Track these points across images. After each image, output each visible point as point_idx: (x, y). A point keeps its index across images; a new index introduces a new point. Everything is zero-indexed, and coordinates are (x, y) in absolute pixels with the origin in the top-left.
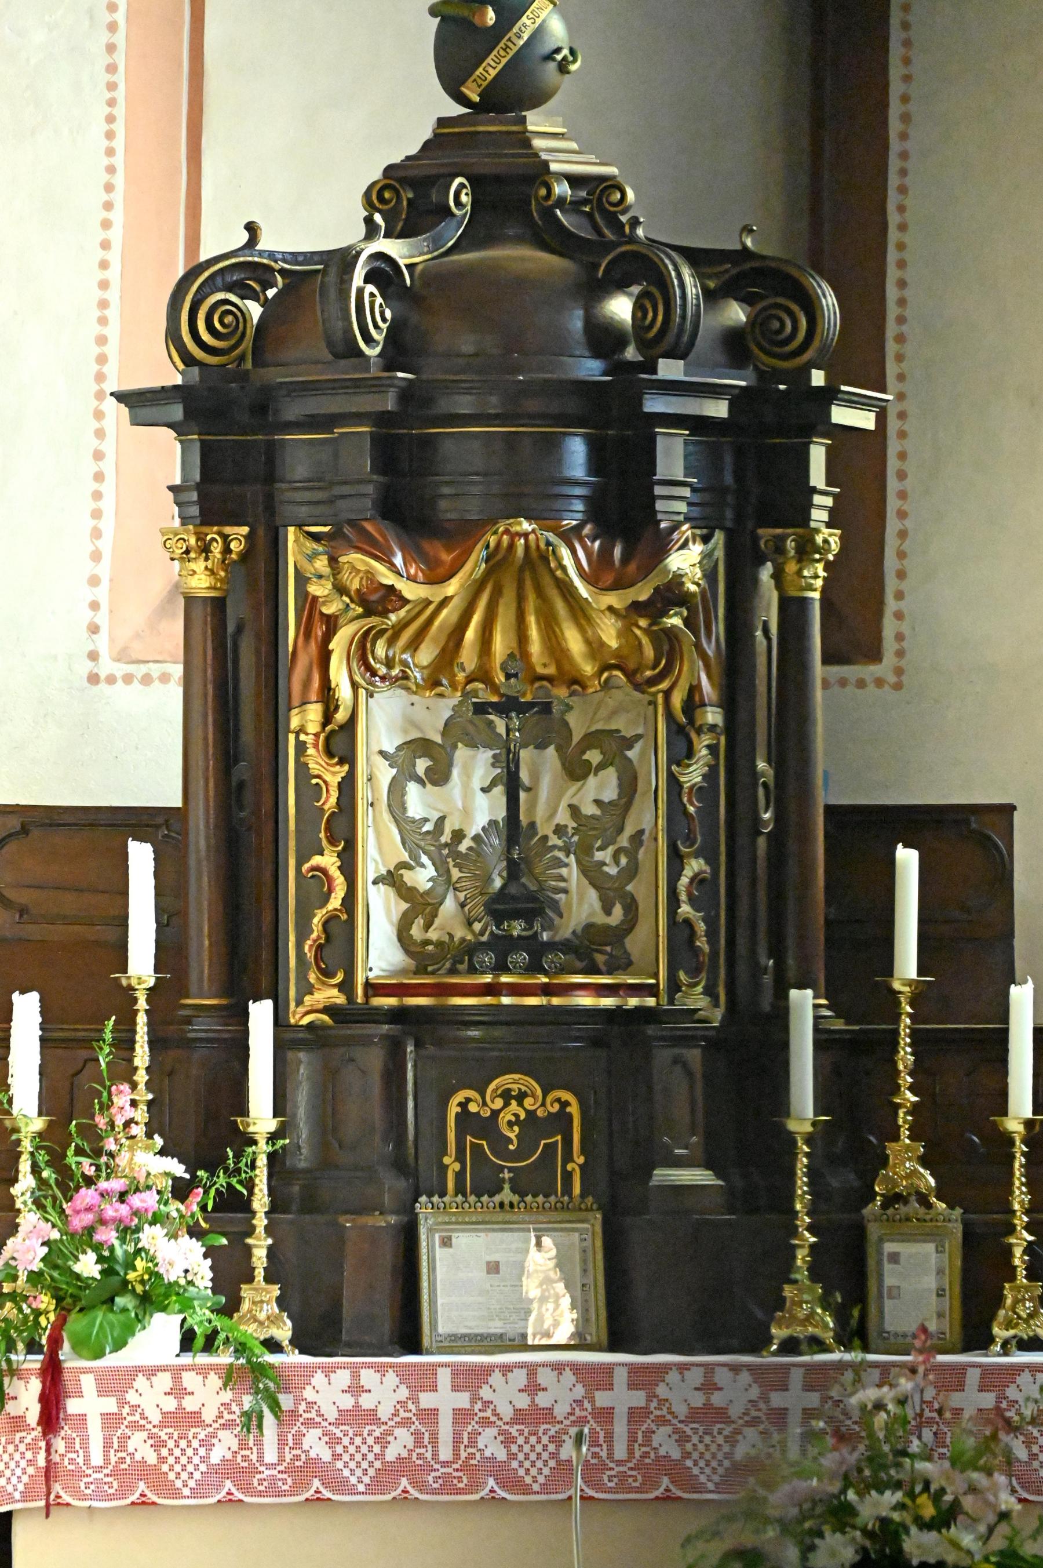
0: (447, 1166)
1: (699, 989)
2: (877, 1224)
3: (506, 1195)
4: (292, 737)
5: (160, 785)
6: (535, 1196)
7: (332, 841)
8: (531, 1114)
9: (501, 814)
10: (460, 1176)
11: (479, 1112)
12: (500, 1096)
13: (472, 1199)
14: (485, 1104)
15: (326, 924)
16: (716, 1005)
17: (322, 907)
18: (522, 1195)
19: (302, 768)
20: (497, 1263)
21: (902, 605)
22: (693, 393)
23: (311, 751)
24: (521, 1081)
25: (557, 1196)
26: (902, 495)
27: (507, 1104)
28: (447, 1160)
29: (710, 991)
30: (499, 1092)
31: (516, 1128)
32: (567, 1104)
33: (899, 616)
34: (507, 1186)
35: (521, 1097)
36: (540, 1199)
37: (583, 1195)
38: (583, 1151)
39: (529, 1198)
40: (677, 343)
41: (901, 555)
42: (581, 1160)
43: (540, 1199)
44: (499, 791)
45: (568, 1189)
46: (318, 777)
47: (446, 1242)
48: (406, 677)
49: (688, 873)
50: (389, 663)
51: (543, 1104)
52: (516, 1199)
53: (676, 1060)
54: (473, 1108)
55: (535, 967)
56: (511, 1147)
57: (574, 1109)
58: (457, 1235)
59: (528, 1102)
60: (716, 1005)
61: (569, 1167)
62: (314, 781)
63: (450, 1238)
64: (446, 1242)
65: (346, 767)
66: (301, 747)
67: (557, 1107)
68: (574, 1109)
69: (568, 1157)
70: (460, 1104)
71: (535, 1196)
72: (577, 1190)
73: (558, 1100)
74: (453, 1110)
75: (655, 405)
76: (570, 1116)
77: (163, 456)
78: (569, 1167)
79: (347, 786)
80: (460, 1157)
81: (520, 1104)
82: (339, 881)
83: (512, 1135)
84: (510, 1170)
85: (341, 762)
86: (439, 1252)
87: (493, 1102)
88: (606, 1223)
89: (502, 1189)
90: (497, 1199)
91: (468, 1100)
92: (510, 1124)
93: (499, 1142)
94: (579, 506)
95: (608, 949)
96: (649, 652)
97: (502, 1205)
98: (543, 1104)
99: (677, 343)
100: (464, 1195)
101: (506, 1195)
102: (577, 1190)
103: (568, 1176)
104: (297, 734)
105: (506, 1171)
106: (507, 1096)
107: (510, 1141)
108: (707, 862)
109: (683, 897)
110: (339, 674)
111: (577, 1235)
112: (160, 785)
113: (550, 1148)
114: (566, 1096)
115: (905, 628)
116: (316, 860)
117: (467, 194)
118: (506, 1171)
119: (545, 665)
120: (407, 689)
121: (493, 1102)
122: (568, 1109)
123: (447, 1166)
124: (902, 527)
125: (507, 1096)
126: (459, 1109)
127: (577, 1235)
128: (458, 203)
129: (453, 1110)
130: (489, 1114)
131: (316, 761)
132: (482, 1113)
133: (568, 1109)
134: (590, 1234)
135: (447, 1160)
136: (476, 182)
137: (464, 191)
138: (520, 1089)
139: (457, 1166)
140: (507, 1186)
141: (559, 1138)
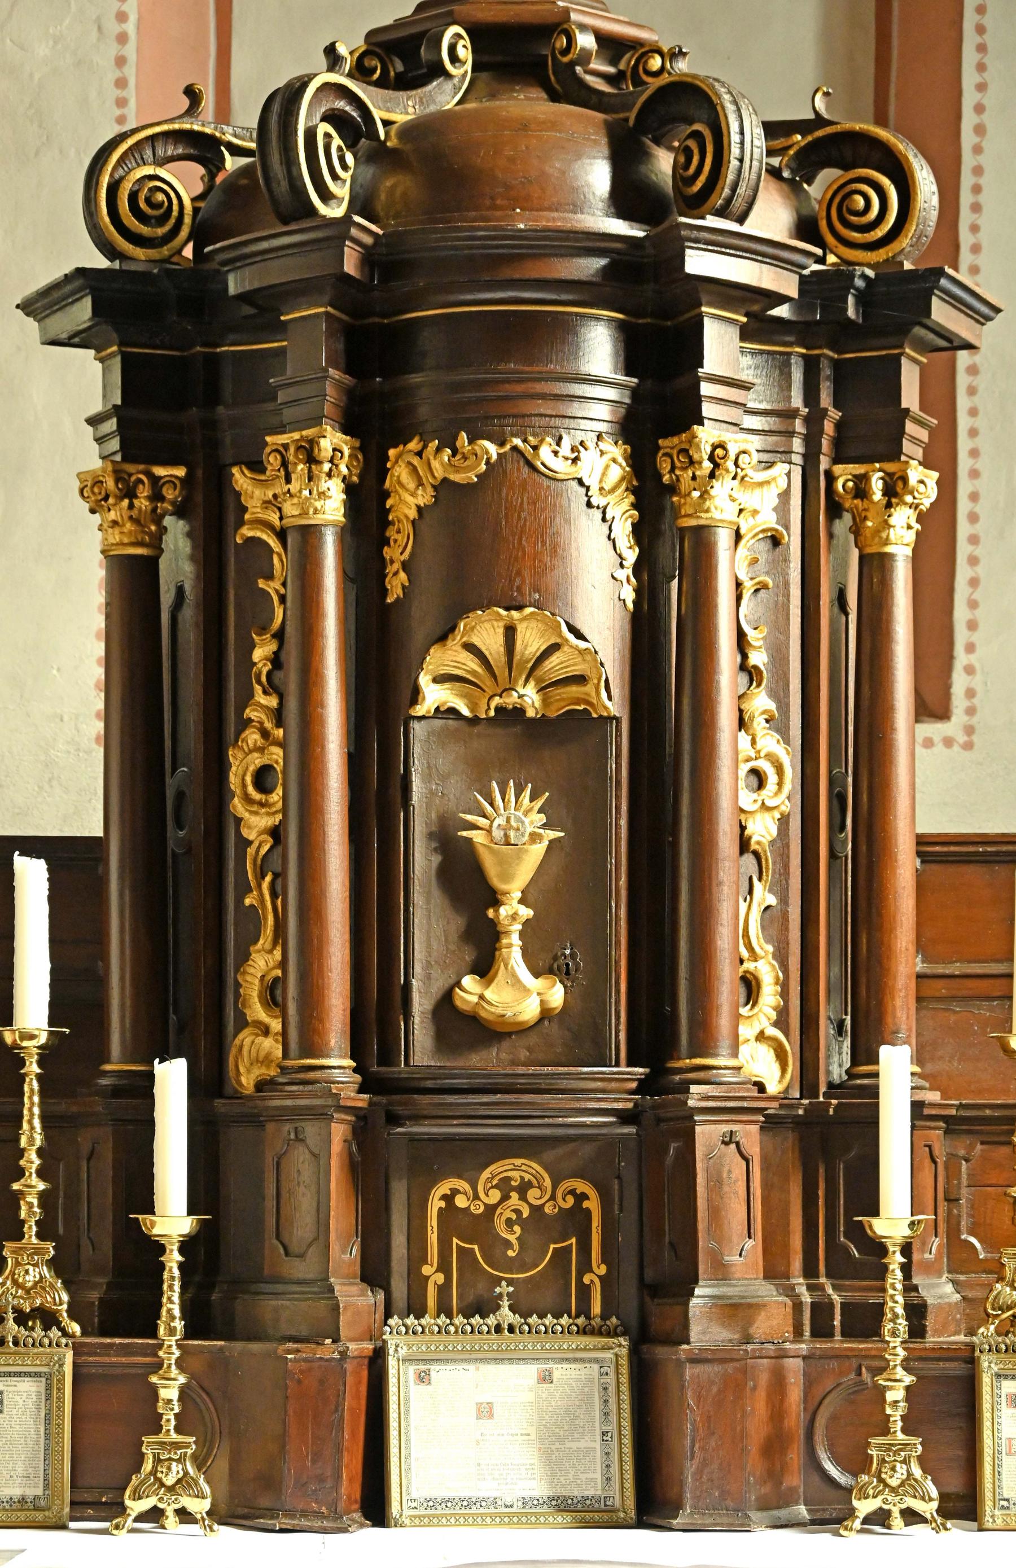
0: (428, 1278)
2: (992, 1357)
3: (506, 1315)
5: (80, 809)
6: (542, 1316)
8: (537, 1210)
10: (444, 1290)
11: (468, 1208)
12: (496, 1187)
13: (459, 1320)
14: (476, 1197)
18: (525, 1315)
20: (491, 1406)
21: (973, 659)
22: (752, 243)
24: (523, 1168)
25: (570, 1317)
26: (974, 540)
27: (505, 1198)
28: (426, 1270)
30: (495, 1182)
31: (517, 1229)
32: (584, 1197)
33: (970, 670)
34: (505, 1303)
35: (523, 1189)
36: (549, 1320)
37: (605, 1316)
39: (534, 1320)
40: (729, 201)
41: (973, 605)
42: (603, 1270)
43: (549, 1320)
45: (584, 1309)
47: (423, 1378)
51: (553, 1198)
52: (516, 1319)
53: (729, 1139)
54: (461, 1202)
56: (511, 1253)
58: (438, 1368)
59: (533, 1194)
61: (586, 1280)
63: (428, 1372)
64: (423, 1378)
67: (570, 1201)
68: (593, 1204)
69: (585, 1266)
70: (444, 1197)
71: (542, 1316)
72: (596, 1308)
73: (572, 1192)
74: (436, 1204)
75: (698, 262)
76: (588, 1212)
77: (87, 380)
78: (586, 1280)
80: (444, 1267)
81: (523, 1198)
83: (512, 1238)
84: (510, 1282)
86: (416, 1392)
87: (487, 1195)
88: (635, 1352)
89: (498, 1307)
90: (492, 1321)
91: (455, 1192)
92: (509, 1223)
93: (494, 1246)
94: (603, 411)
97: (498, 1329)
98: (553, 1198)
99: (729, 201)
100: (449, 1316)
101: (506, 1315)
102: (596, 1308)
103: (584, 1292)
105: (504, 1283)
106: (504, 1186)
107: (508, 1244)
111: (596, 1367)
112: (80, 809)
113: (562, 1255)
114: (582, 1186)
115: (977, 682)
117: (464, 46)
118: (504, 1283)
121: (487, 1195)
122: (586, 1204)
123: (428, 1278)
124: (974, 575)
125: (504, 1186)
126: (443, 1204)
127: (596, 1367)
128: (454, 59)
129: (436, 1204)
130: (482, 1208)
132: (472, 1208)
133: (586, 1204)
134: (613, 1366)
135: (426, 1270)
136: (477, 33)
137: (461, 43)
138: (522, 1178)
139: (440, 1278)
140: (505, 1303)
141: (574, 1240)
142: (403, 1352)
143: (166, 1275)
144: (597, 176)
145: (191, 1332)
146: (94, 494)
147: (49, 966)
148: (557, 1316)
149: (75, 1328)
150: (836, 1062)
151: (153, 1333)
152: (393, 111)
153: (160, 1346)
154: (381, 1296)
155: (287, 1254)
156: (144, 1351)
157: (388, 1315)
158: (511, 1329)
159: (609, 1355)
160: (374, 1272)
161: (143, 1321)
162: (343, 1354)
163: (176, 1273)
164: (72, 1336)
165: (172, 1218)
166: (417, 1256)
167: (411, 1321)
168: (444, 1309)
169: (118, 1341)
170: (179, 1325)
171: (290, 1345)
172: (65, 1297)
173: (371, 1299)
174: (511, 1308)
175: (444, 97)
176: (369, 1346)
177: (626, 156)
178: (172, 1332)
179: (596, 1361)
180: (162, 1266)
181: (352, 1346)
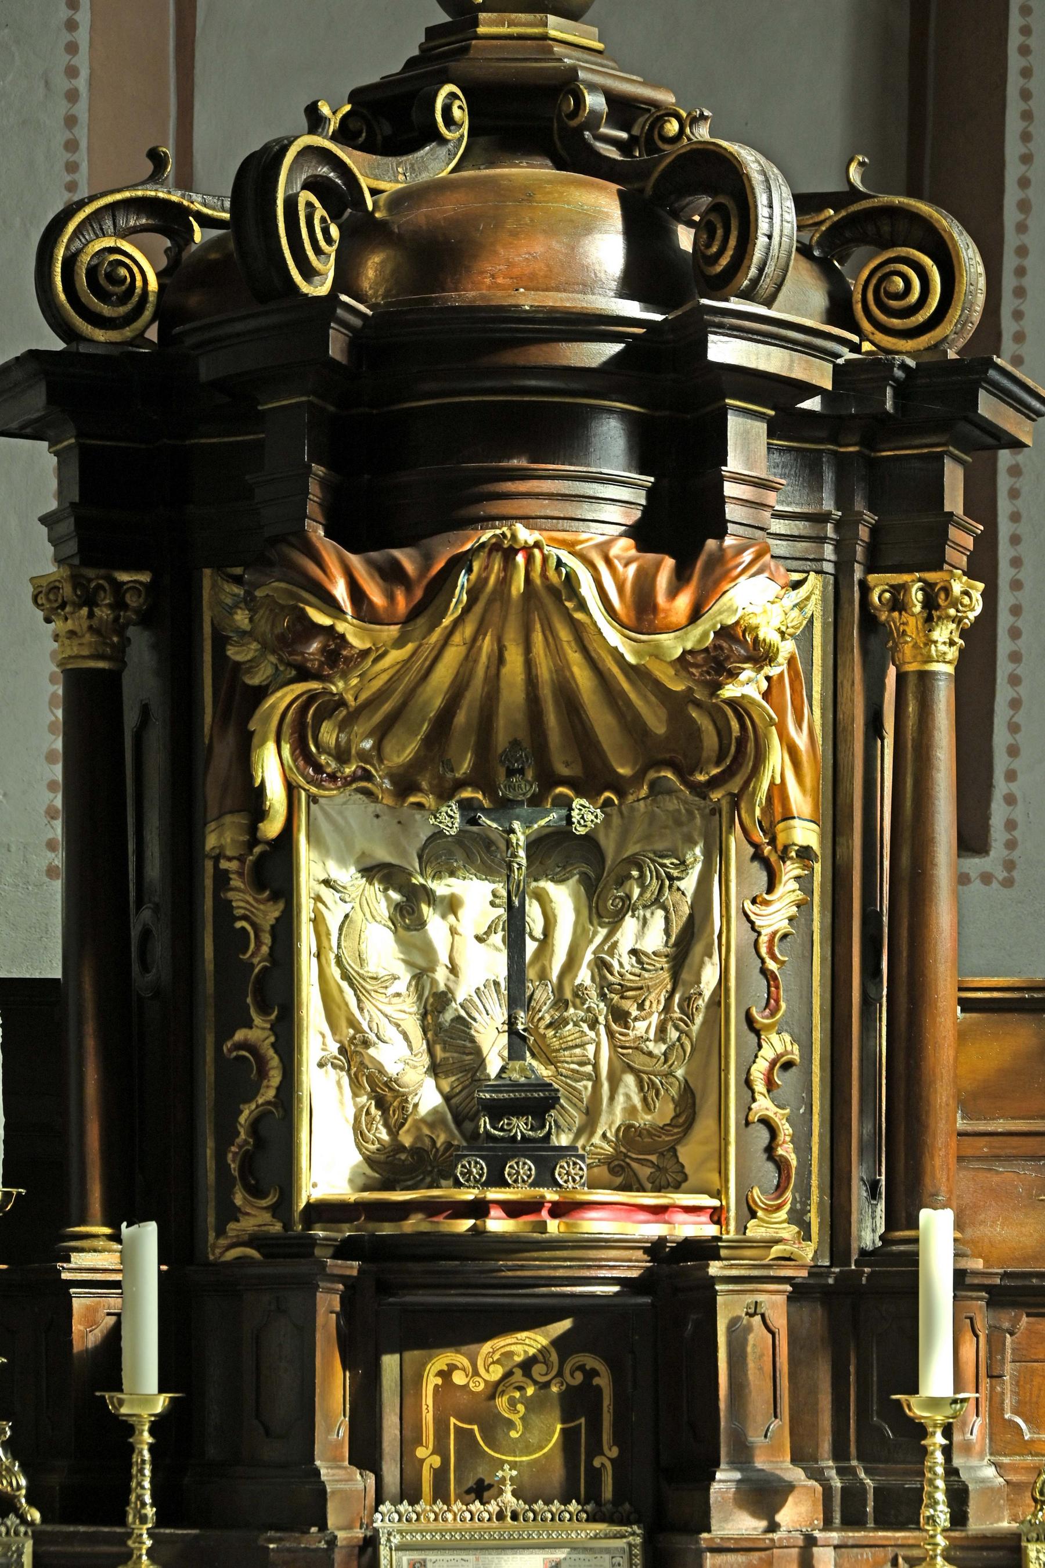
0: (422, 1461)
1: (783, 1215)
4: (209, 865)
6: (548, 1502)
7: (264, 1009)
9: (501, 972)
11: (466, 1386)
12: (498, 1362)
13: (457, 1506)
14: (476, 1373)
15: (255, 1127)
16: (808, 1237)
17: (248, 1100)
18: (530, 1501)
19: (224, 910)
21: (1014, 787)
23: (236, 882)
24: (527, 1341)
25: (578, 1503)
28: (421, 1452)
29: (798, 1218)
30: (496, 1357)
31: (520, 1407)
32: (594, 1373)
33: (1010, 800)
34: (509, 1488)
38: (618, 1440)
39: (539, 1506)
40: (755, 282)
41: (1014, 728)
42: (614, 1452)
44: (497, 939)
46: (245, 918)
48: (367, 776)
49: (767, 1053)
50: (342, 756)
51: (560, 1374)
52: (521, 1506)
54: (459, 1378)
55: (546, 1177)
56: (514, 1434)
57: (604, 1381)
58: (434, 1558)
59: (537, 1370)
60: (808, 1237)
61: (597, 1463)
62: (239, 924)
65: (281, 905)
66: (222, 879)
67: (579, 1377)
68: (604, 1381)
69: (595, 1448)
70: (440, 1373)
71: (548, 1502)
72: (608, 1492)
73: (581, 1368)
74: (431, 1381)
75: (722, 350)
76: (599, 1390)
78: (597, 1463)
79: (285, 933)
80: (440, 1448)
82: (274, 1061)
83: (515, 1418)
84: (513, 1465)
85: (274, 897)
87: (488, 1371)
89: (501, 1492)
90: (493, 1507)
91: (452, 1368)
93: (493, 1426)
95: (653, 1158)
96: (710, 740)
97: (500, 1516)
100: (446, 1501)
102: (608, 1492)
103: (595, 1476)
104: (217, 859)
105: (506, 1467)
107: (510, 1424)
108: (795, 1040)
109: (760, 1087)
110: (271, 767)
111: (607, 1557)
114: (591, 1362)
115: (1018, 813)
116: (240, 1035)
117: (460, 107)
118: (506, 1467)
119: (567, 765)
120: (368, 793)
121: (488, 1371)
122: (596, 1381)
123: (422, 1461)
124: (1015, 695)
126: (439, 1381)
127: (607, 1557)
128: (449, 120)
129: (431, 1381)
130: (482, 1386)
131: (242, 897)
132: (471, 1385)
133: (596, 1381)
134: (626, 1556)
135: (421, 1452)
136: (474, 93)
138: (525, 1352)
139: (436, 1461)
140: (509, 1488)
141: (583, 1420)
142: (396, 1540)
143: (135, 1458)
144: (607, 251)
145: (161, 1520)
146: (49, 599)
147: (3, 1120)
148: (565, 1502)
149: (35, 1515)
150: (869, 1230)
151: (122, 1521)
152: (380, 179)
153: (129, 1535)
154: (371, 1479)
155: (268, 1433)
156: (109, 1539)
157: (379, 1500)
158: (515, 1516)
159: (621, 1543)
160: (365, 1452)
161: (114, 1506)
162: (332, 1542)
163: (147, 1455)
164: (32, 1523)
165: (144, 1393)
166: (410, 1440)
167: (404, 1507)
168: (440, 1493)
169: (82, 1529)
170: (150, 1511)
171: (271, 1534)
172: (23, 1482)
173: (363, 1482)
174: (514, 1493)
175: (436, 164)
176: (359, 1533)
177: (644, 231)
178: (143, 1519)
179: (607, 1550)
180: (131, 1449)
181: (341, 1535)
